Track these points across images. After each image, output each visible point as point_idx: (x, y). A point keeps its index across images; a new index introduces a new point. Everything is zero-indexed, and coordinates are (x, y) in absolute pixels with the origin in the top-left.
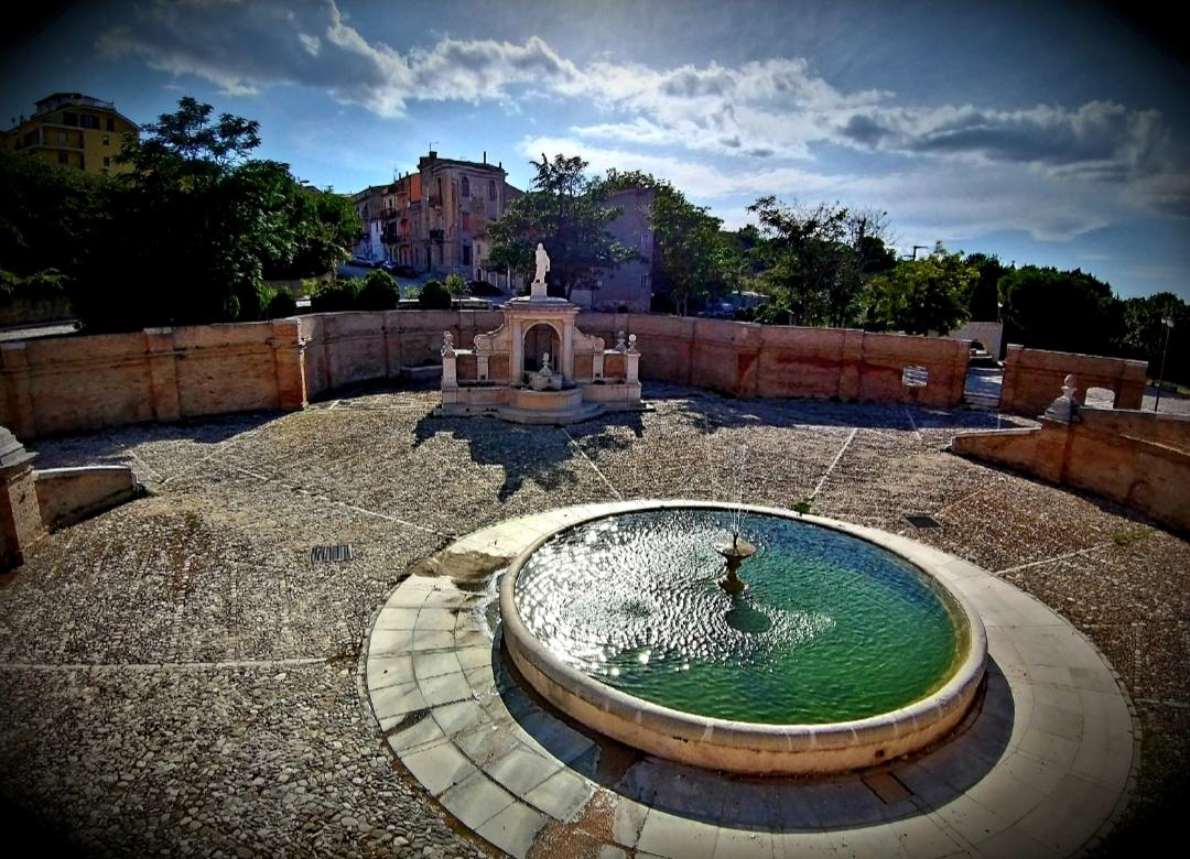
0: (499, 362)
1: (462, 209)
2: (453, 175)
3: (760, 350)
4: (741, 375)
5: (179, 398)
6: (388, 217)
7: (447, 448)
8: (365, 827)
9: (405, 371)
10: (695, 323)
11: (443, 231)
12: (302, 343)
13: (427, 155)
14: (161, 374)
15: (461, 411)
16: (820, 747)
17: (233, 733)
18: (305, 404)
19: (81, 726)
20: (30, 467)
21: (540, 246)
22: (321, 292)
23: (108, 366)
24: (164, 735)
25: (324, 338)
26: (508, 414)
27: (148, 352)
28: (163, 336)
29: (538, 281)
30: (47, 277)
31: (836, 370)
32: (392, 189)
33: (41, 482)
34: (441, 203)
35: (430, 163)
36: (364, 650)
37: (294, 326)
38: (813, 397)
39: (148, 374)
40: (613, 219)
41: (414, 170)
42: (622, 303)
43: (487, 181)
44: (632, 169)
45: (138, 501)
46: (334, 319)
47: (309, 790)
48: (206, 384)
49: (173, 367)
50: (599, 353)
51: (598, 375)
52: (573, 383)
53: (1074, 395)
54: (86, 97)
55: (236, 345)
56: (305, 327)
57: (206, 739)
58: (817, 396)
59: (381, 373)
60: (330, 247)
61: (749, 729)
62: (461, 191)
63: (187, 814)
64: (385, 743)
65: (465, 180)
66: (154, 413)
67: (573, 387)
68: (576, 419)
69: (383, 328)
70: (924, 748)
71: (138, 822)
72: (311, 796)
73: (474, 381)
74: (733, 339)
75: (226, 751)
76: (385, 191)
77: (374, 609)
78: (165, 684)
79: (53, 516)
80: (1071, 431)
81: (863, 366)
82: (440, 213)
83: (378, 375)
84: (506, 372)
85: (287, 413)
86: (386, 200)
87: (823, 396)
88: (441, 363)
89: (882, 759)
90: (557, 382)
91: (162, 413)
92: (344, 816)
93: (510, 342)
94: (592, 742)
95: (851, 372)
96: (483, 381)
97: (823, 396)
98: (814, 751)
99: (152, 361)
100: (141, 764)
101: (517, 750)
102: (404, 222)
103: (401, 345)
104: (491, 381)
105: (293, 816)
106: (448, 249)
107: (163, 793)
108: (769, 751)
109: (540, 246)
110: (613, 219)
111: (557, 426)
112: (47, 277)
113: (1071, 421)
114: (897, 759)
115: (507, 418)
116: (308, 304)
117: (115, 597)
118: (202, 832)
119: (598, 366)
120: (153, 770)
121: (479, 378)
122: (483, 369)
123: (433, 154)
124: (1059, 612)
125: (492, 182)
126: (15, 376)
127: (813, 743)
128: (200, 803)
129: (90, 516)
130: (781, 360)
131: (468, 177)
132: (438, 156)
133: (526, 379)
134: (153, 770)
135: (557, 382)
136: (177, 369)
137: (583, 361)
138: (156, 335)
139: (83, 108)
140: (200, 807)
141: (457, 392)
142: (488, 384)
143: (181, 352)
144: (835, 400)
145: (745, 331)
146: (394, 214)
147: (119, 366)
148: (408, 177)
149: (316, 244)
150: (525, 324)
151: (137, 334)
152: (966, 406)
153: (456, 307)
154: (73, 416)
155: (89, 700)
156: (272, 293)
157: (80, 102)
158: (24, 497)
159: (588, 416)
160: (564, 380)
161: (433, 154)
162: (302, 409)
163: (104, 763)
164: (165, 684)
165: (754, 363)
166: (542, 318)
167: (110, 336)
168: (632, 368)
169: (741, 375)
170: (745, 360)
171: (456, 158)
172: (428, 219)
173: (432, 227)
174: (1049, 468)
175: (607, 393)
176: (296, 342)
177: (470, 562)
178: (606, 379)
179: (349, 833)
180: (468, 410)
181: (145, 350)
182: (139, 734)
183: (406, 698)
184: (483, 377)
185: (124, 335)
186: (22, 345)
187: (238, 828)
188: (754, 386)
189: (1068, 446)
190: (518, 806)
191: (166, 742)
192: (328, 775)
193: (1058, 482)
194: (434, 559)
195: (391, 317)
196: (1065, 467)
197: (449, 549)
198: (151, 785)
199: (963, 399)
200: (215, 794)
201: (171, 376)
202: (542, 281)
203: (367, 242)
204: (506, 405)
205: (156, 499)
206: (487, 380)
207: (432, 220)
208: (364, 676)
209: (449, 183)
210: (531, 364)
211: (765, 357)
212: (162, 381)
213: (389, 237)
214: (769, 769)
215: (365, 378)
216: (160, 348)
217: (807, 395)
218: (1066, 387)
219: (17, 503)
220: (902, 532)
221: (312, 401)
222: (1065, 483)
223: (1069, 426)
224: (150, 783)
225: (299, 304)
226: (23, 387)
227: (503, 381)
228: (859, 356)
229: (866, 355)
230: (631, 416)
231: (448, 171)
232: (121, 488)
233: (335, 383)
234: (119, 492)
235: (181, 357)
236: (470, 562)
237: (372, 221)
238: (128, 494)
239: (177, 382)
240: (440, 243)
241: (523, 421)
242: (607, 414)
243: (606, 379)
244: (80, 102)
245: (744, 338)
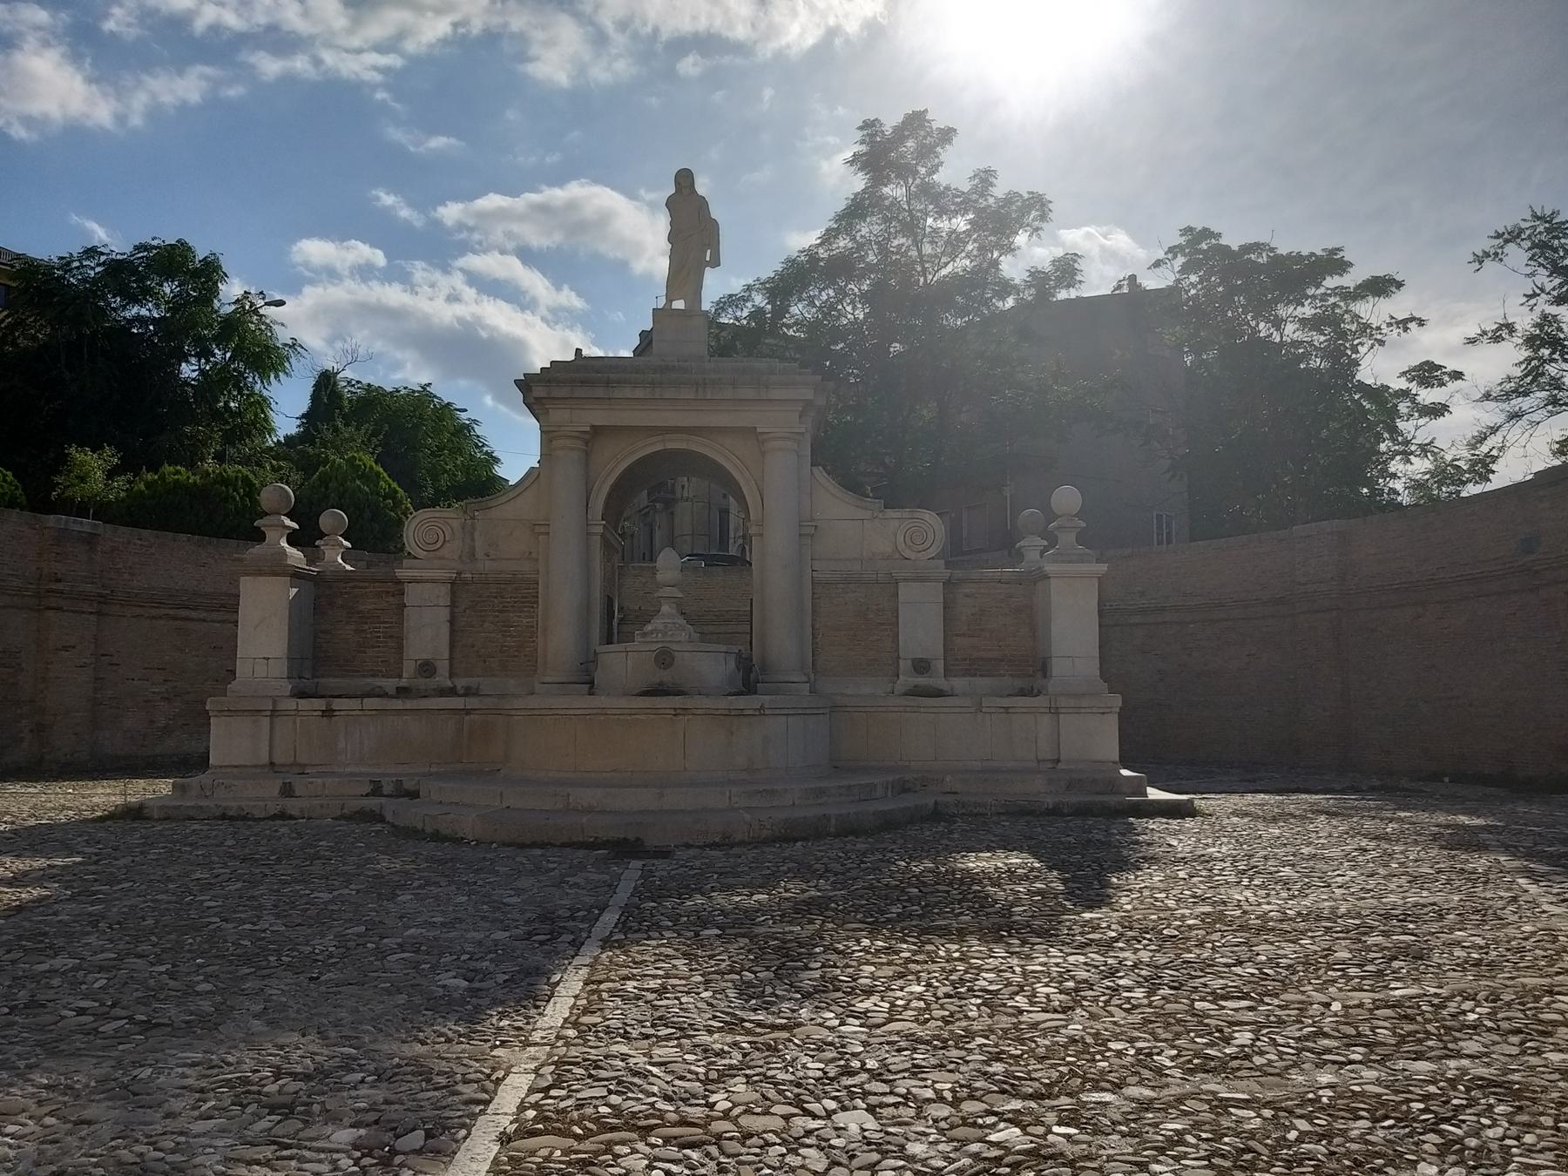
51: (921, 666)
73: (390, 684)
96: (422, 682)
121: (409, 668)
133: (586, 678)
141: (274, 713)
142: (451, 692)
178: (959, 683)
180: (287, 791)
184: (427, 668)
206: (442, 679)
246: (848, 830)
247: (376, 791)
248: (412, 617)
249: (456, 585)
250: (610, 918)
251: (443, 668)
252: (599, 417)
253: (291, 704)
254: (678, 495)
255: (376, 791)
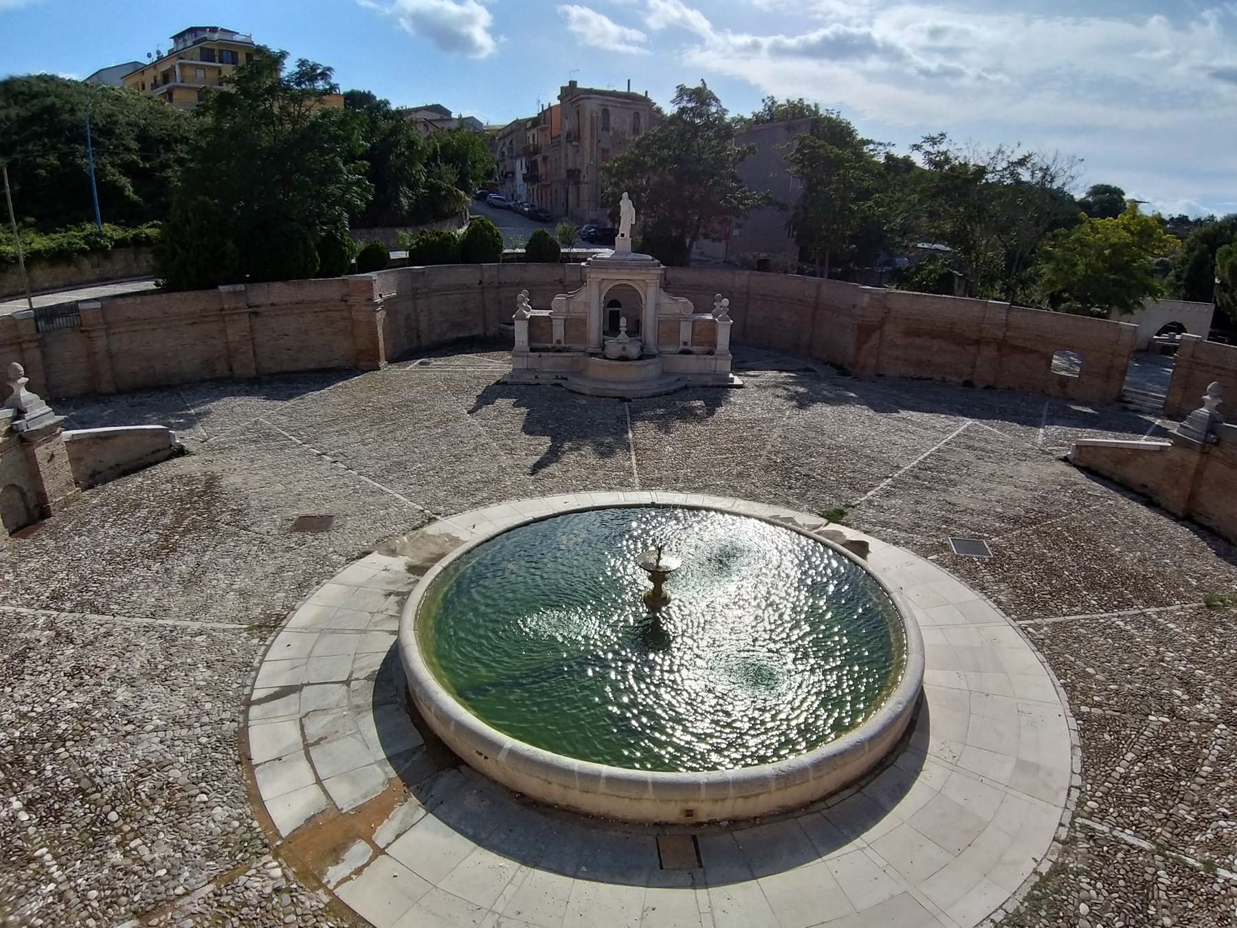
0: (575, 325)
1: (602, 145)
2: (592, 106)
3: (883, 322)
4: (859, 349)
5: (255, 354)
6: (531, 153)
7: (509, 413)
8: (184, 780)
9: (503, 329)
10: (819, 286)
11: (579, 171)
12: (378, 300)
13: (567, 84)
14: (236, 331)
15: (529, 378)
16: (608, 791)
17: (134, 684)
18: (383, 363)
19: (27, 663)
20: (60, 429)
21: (625, 195)
22: (417, 243)
23: (184, 323)
24: (82, 678)
25: (412, 294)
26: (576, 383)
27: (222, 310)
28: (235, 293)
29: (622, 235)
30: (148, 231)
31: (972, 349)
32: (535, 122)
33: (72, 442)
34: (578, 138)
35: (571, 93)
36: (283, 623)
37: (370, 284)
38: (943, 380)
39: (223, 331)
40: (742, 159)
41: (558, 102)
42: (763, 256)
43: (632, 112)
44: (795, 99)
45: (175, 460)
46: (423, 273)
47: (161, 742)
48: (282, 341)
49: (248, 324)
50: (686, 319)
51: (685, 344)
52: (655, 351)
53: (1217, 408)
54: (222, 30)
55: (313, 302)
56: (383, 285)
57: (111, 686)
58: (948, 378)
59: (478, 331)
60: (449, 190)
61: (547, 759)
62: (600, 126)
63: (64, 746)
64: (246, 713)
65: (606, 112)
66: (231, 370)
67: (653, 356)
68: (645, 393)
69: (481, 283)
70: (755, 818)
71: (27, 746)
72: (161, 746)
73: (549, 345)
74: (854, 306)
75: (120, 699)
76: (529, 125)
77: (318, 583)
78: (108, 634)
79: (89, 472)
80: (1204, 453)
81: (1005, 346)
82: (577, 150)
83: (476, 332)
84: (583, 338)
85: (363, 372)
86: (530, 134)
87: (956, 379)
88: (513, 324)
89: (691, 820)
90: (634, 350)
91: (238, 371)
92: (175, 768)
93: (587, 304)
94: (421, 741)
95: (989, 352)
96: (559, 346)
97: (956, 379)
98: (602, 794)
99: (227, 318)
100: (53, 700)
101: (350, 737)
102: (545, 159)
103: (500, 302)
104: (567, 345)
105: (137, 761)
106: (585, 191)
107: (56, 726)
108: (560, 785)
109: (625, 195)
110: (742, 159)
111: (622, 399)
112: (148, 231)
113: (1205, 441)
114: (712, 823)
115: (574, 388)
116: (404, 255)
117: (110, 552)
118: (66, 761)
119: (685, 333)
120: (59, 706)
121: (554, 342)
122: (558, 332)
123: (573, 84)
124: (1064, 686)
125: (638, 113)
126: (93, 334)
127: (602, 787)
128: (77, 738)
129: (126, 473)
130: (909, 333)
131: (609, 108)
132: (579, 86)
134: (59, 706)
135: (634, 350)
136: (251, 327)
137: (669, 328)
138: (229, 293)
139: (220, 42)
140: (76, 741)
143: (256, 309)
144: (968, 384)
145: (866, 298)
146: (537, 151)
147: (195, 323)
148: (550, 108)
149: (434, 189)
150: (605, 283)
151: (211, 292)
152: (1124, 404)
153: (568, 258)
154: (151, 371)
155: (44, 641)
156: (360, 245)
157: (216, 36)
158: (52, 456)
159: (659, 390)
160: (642, 349)
161: (573, 84)
162: (378, 369)
163: (28, 696)
164: (108, 634)
165: (877, 334)
166: (623, 276)
167: (184, 294)
168: (723, 338)
169: (859, 349)
170: (865, 331)
171: (597, 87)
172: (566, 156)
173: (570, 166)
174: (1175, 496)
175: (691, 364)
176: (371, 299)
177: (437, 544)
179: (169, 783)
180: (536, 377)
181: (220, 307)
182: (65, 674)
183: (290, 672)
184: (559, 342)
185: (198, 293)
186: (98, 305)
187: (92, 763)
188: (874, 362)
189: (1199, 472)
190: (317, 789)
191: (81, 685)
192: (184, 732)
193: (1181, 514)
194: (405, 539)
195: (489, 270)
196: (1192, 497)
197: (424, 529)
198: (51, 719)
199: (1120, 399)
200: (93, 733)
201: (245, 334)
202: (627, 235)
203: (512, 181)
204: (578, 374)
205: (194, 458)
206: (563, 345)
207: (570, 158)
208: (269, 647)
209: (588, 115)
210: (612, 327)
211: (889, 329)
212: (237, 338)
213: (532, 177)
214: (565, 803)
215: (460, 335)
216: (233, 305)
217: (938, 377)
218: (1207, 397)
219: (45, 462)
220: (935, 557)
221: (391, 361)
222: (1187, 518)
223: (1203, 447)
224: (51, 715)
225: (394, 255)
226: (100, 344)
227: (581, 347)
228: (1000, 334)
229: (1008, 334)
230: (716, 392)
231: (587, 102)
232: (160, 447)
233: (425, 342)
234: (159, 450)
235: (256, 314)
236: (437, 544)
237: (518, 156)
238: (167, 453)
239: (253, 339)
240: (577, 183)
241: (587, 392)
242: (686, 388)
243: (694, 348)
244: (216, 36)
245: (865, 306)
246: (667, 394)
247: (557, 378)
248: (554, 329)
249: (565, 320)
250: (629, 419)
251: (563, 341)
252: (604, 276)
253: (531, 354)
254: (582, 180)
255: (557, 378)
